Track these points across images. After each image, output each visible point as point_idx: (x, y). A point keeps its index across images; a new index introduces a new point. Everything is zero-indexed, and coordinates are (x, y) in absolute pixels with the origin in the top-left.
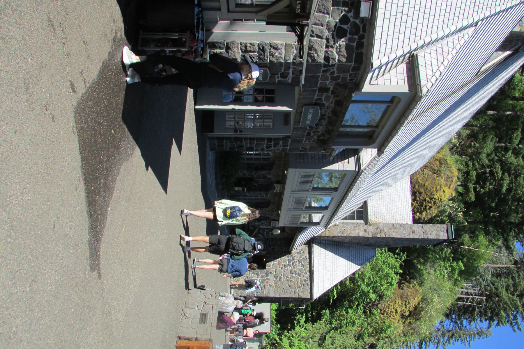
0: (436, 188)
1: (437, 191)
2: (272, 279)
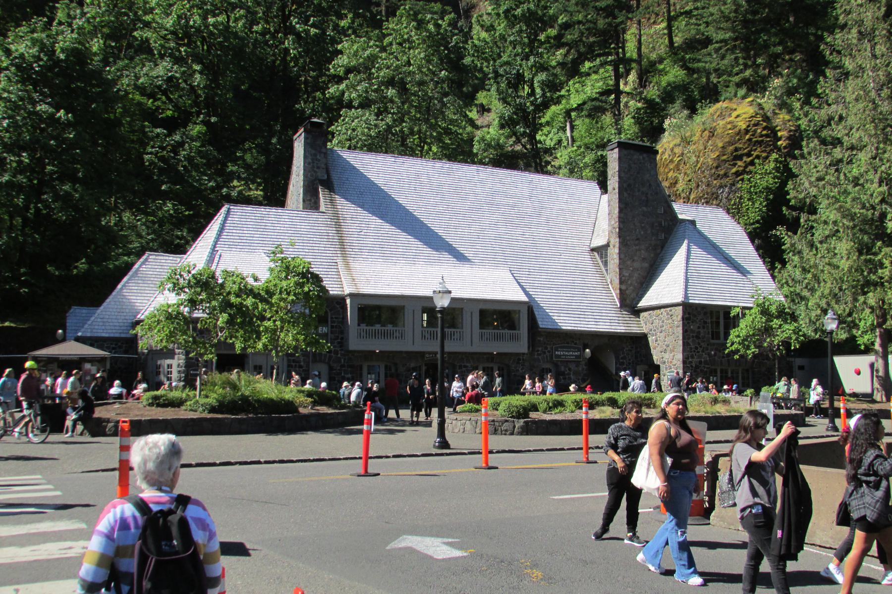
0: (730, 129)
1: (735, 127)
2: (667, 356)
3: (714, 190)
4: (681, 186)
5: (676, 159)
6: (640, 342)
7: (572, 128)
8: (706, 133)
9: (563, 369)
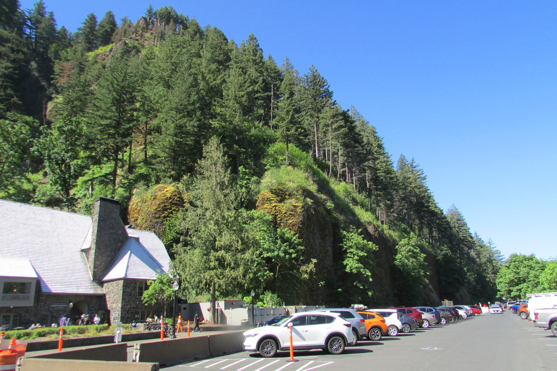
1: (165, 196)
2: (114, 305)
3: (153, 224)
4: (139, 221)
5: (138, 208)
6: (101, 298)
7: (93, 189)
8: (153, 197)
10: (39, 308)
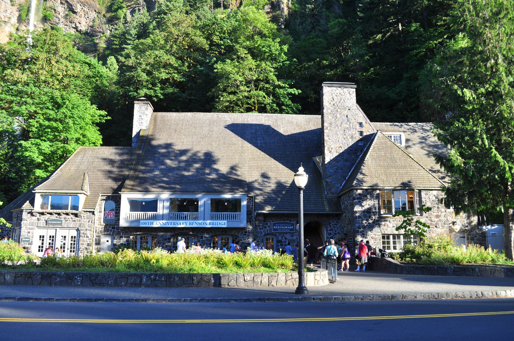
9: (280, 238)
10: (259, 230)
